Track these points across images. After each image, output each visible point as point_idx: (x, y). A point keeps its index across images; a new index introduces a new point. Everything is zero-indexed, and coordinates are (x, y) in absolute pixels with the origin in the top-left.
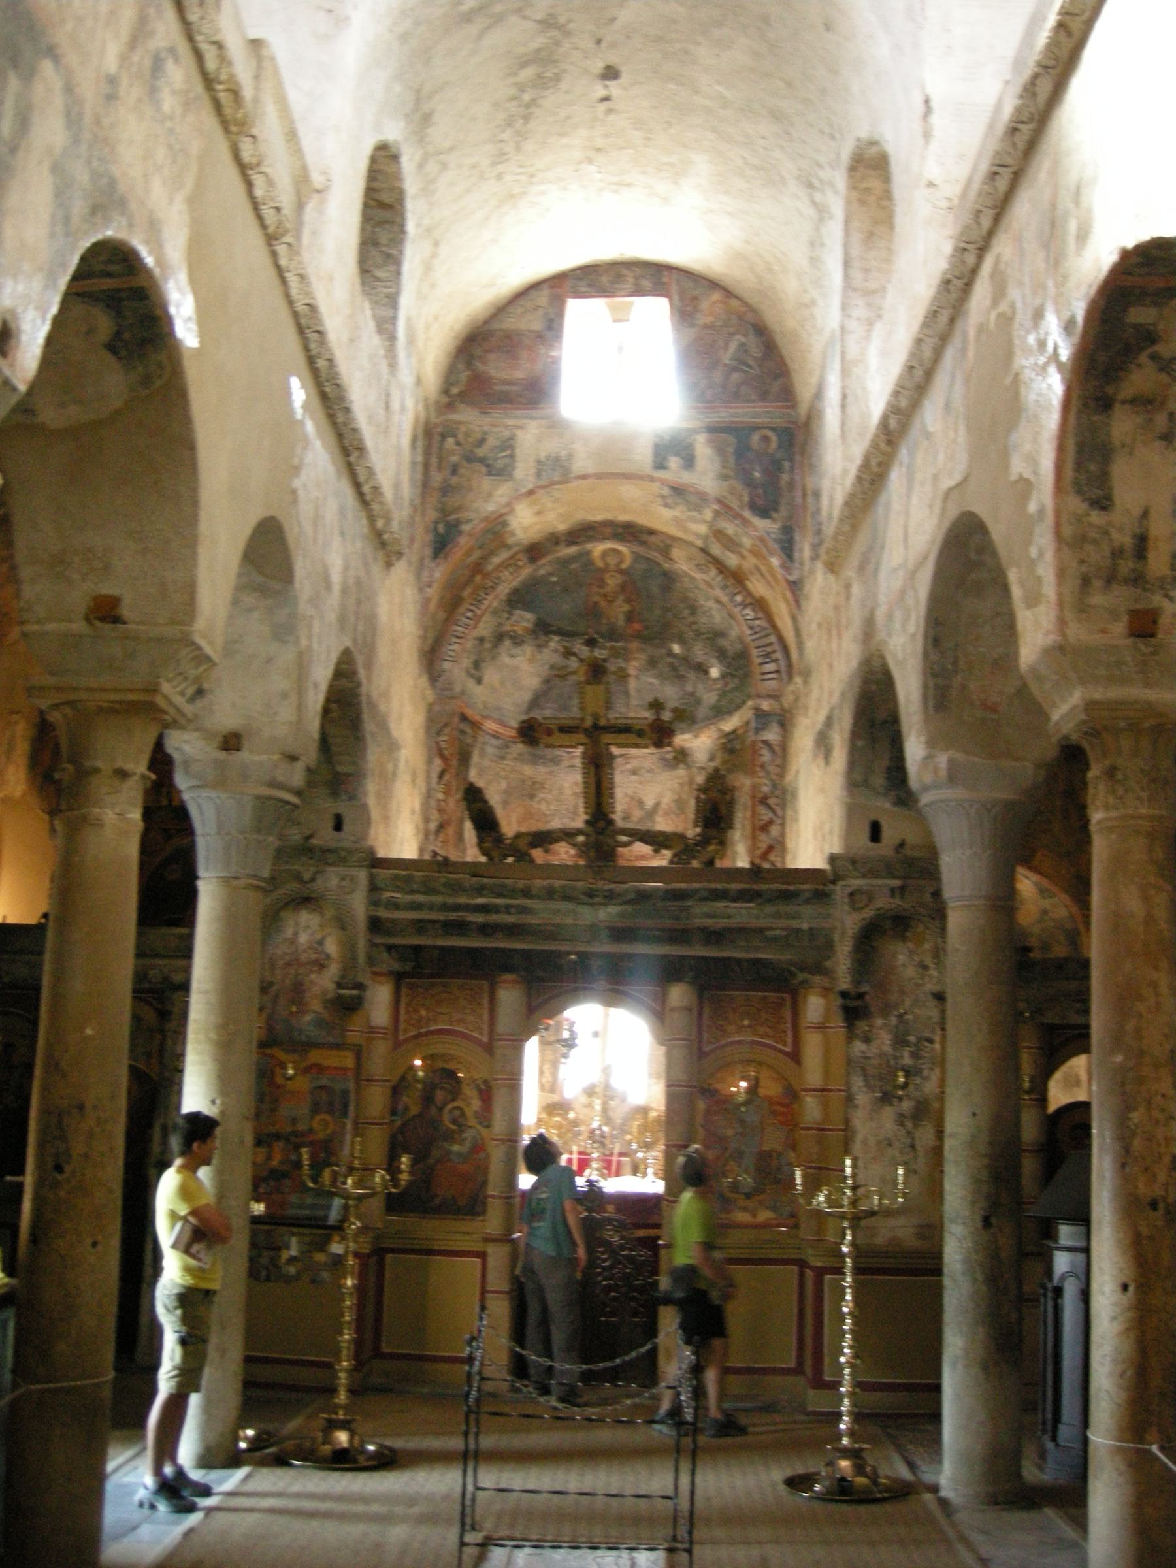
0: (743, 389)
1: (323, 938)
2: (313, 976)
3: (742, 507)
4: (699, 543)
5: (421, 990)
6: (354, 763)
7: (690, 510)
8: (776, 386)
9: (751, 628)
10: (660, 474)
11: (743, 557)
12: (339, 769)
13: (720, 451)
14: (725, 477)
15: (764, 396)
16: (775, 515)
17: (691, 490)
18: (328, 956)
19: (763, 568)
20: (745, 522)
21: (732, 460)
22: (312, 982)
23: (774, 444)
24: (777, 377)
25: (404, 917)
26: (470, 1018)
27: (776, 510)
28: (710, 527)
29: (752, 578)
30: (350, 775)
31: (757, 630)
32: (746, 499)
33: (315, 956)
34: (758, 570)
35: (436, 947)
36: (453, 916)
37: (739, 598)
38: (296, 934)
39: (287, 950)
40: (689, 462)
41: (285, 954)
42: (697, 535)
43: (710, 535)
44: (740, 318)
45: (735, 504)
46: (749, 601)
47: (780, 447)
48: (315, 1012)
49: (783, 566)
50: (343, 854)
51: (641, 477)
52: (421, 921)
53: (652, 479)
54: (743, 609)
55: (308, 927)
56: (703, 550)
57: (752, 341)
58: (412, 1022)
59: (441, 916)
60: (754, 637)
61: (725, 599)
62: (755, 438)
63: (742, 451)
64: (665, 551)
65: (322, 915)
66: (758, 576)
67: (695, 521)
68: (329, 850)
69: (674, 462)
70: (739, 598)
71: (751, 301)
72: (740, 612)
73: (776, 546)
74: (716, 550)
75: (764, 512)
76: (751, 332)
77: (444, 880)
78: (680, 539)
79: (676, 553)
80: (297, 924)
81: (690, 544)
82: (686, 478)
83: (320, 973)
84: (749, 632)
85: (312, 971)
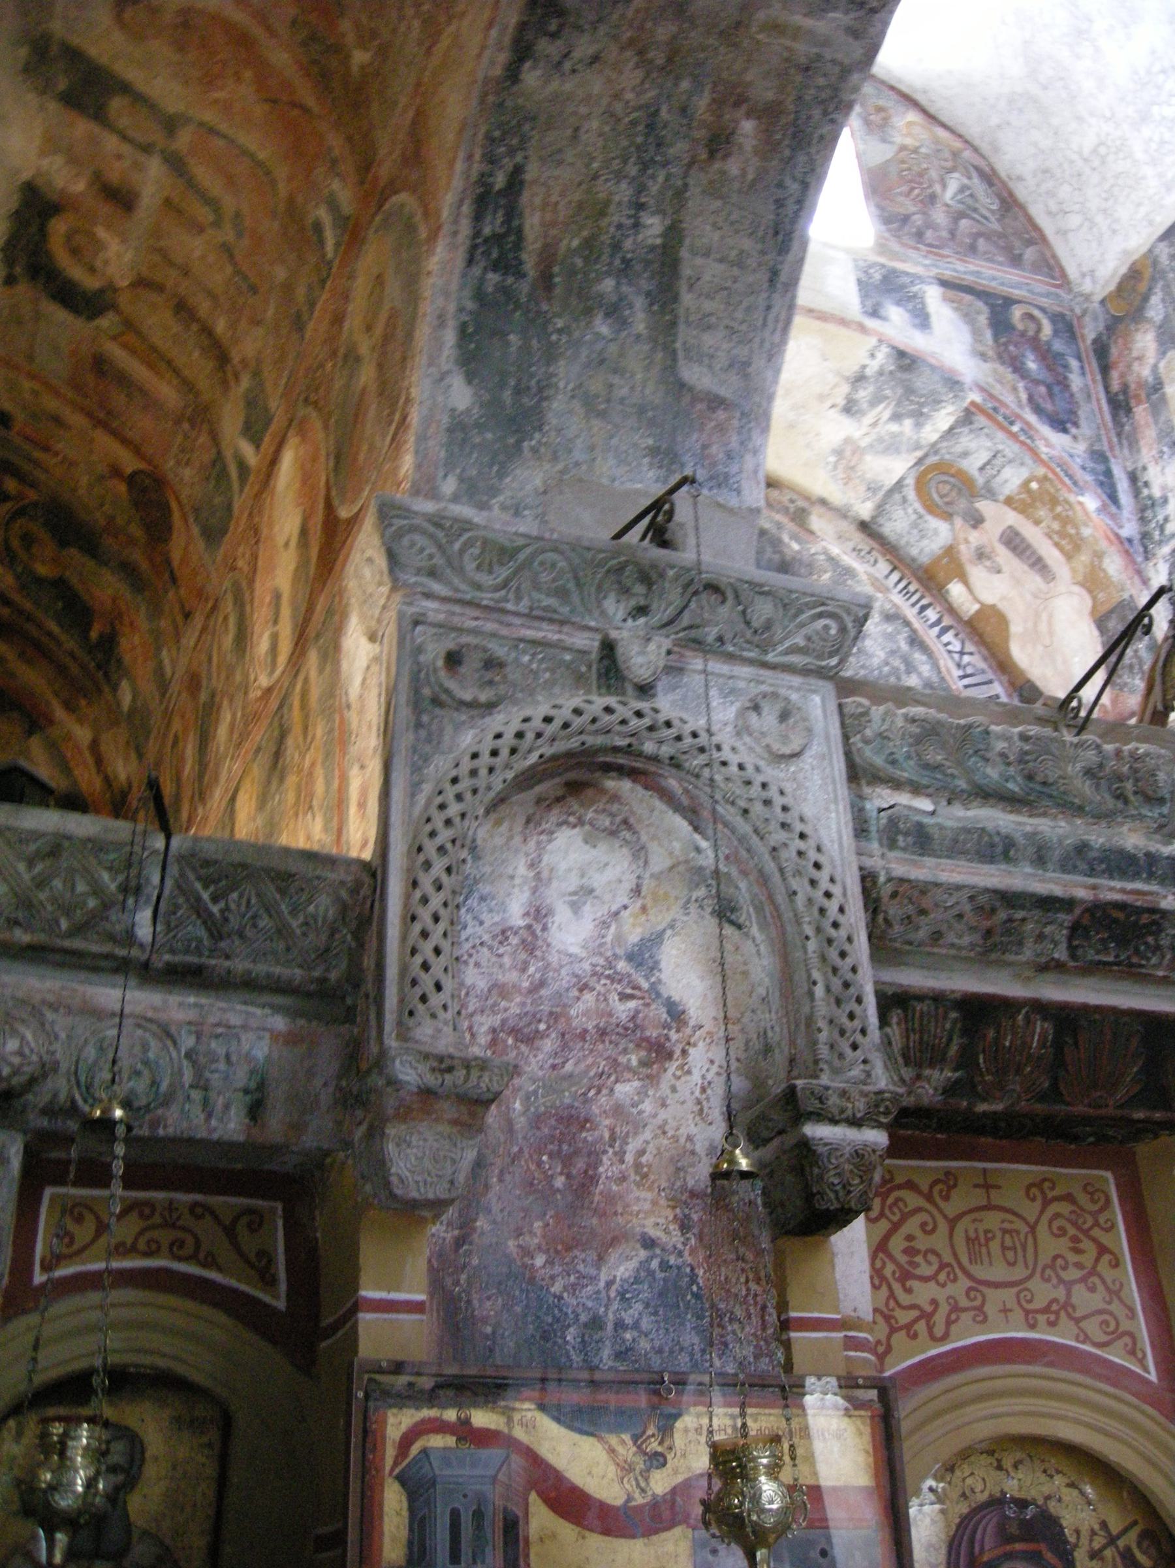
0: (981, 242)
1: (654, 940)
2: (625, 1090)
3: (1021, 406)
4: (865, 510)
5: (913, 1200)
6: (742, 367)
7: (896, 417)
8: (1030, 254)
9: (959, 666)
10: (871, 323)
11: (977, 521)
12: (695, 375)
13: (968, 317)
14: (983, 356)
15: (1016, 260)
16: (1074, 431)
17: (933, 361)
18: (677, 1014)
19: (1033, 534)
20: (1027, 429)
21: (988, 335)
22: (618, 1110)
23: (1047, 330)
24: (1030, 242)
25: (957, 878)
26: (1085, 1299)
27: (1076, 424)
28: (920, 461)
29: (977, 574)
30: (716, 402)
31: (969, 670)
32: (1024, 396)
33: (623, 1010)
34: (1014, 542)
35: (1039, 1007)
36: (1113, 890)
37: (932, 615)
38: (539, 914)
39: (512, 977)
40: (922, 319)
41: (502, 990)
42: (872, 489)
43: (910, 481)
44: (955, 154)
45: (1009, 399)
46: (947, 621)
47: (1056, 333)
48: (649, 1243)
49: (1103, 509)
50: (763, 610)
51: (843, 322)
52: (1009, 898)
53: (862, 329)
54: (939, 636)
55: (588, 892)
56: (864, 526)
57: (978, 186)
58: (903, 1317)
59: (1078, 887)
60: (966, 681)
61: (911, 613)
62: (1017, 313)
63: (1000, 323)
64: (800, 517)
65: (639, 853)
66: (1003, 555)
67: (890, 446)
68: (713, 588)
69: (896, 314)
70: (932, 615)
71: (973, 131)
72: (939, 636)
73: (1089, 478)
74: (896, 525)
75: (1060, 424)
76: (974, 174)
77: (1091, 756)
78: (823, 502)
79: (818, 522)
80: (539, 881)
81: (842, 513)
82: (917, 341)
83: (652, 1080)
84: (958, 673)
85: (616, 1069)
